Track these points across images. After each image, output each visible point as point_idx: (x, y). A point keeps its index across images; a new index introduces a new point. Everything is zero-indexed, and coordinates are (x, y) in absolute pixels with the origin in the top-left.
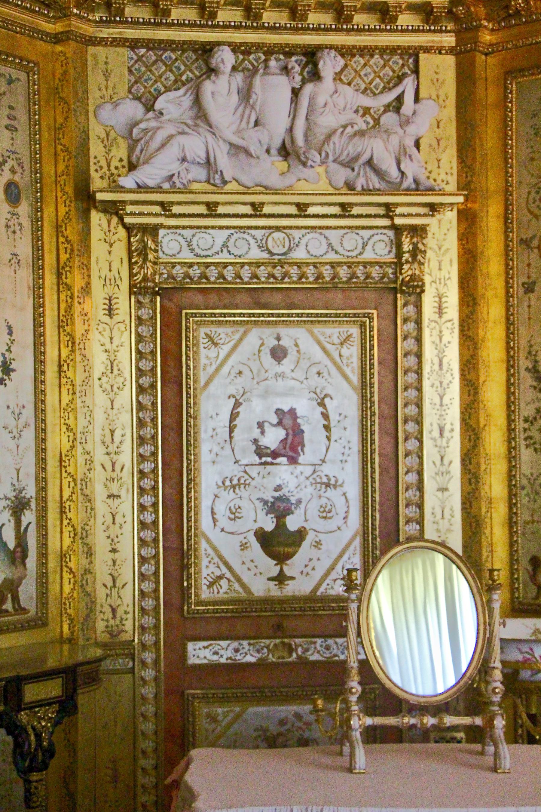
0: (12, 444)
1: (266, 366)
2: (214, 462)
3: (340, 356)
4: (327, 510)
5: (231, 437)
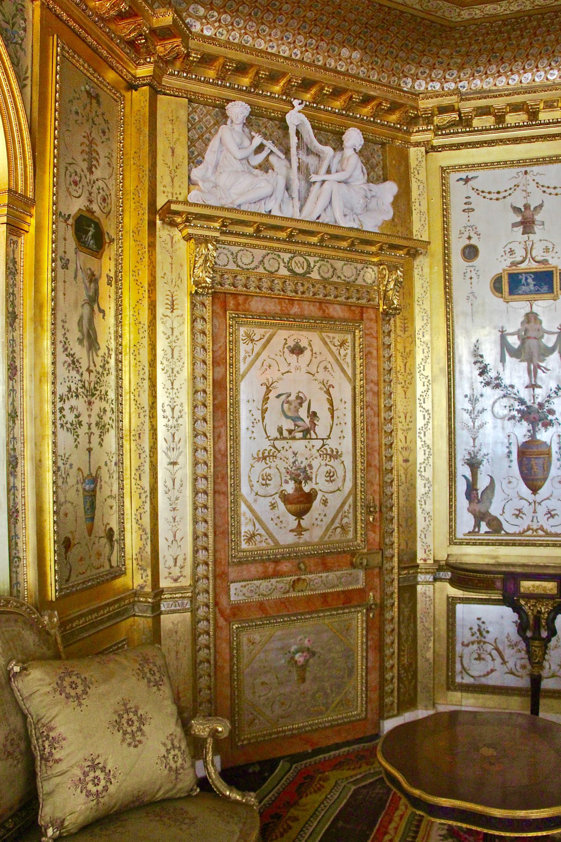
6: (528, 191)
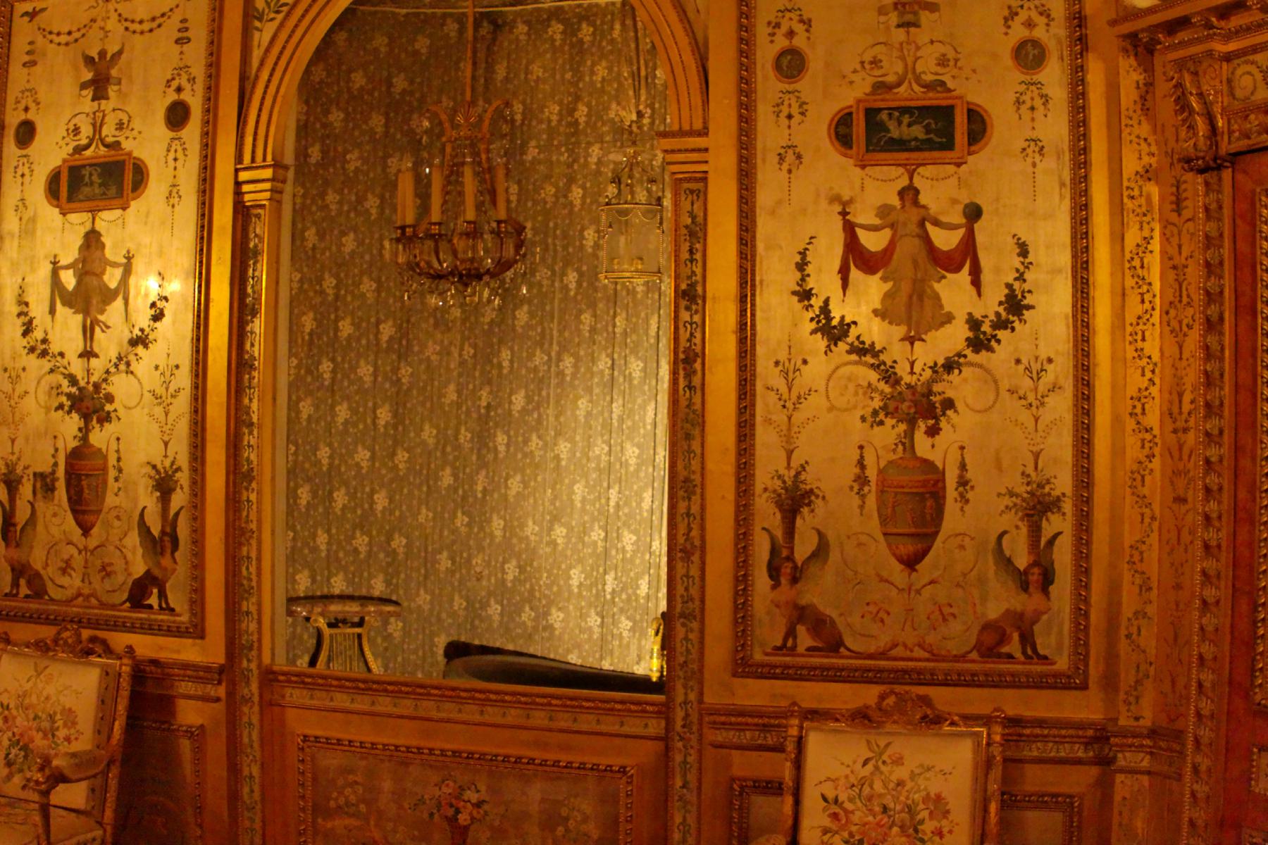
0: (1025, 417)
6: (108, 28)
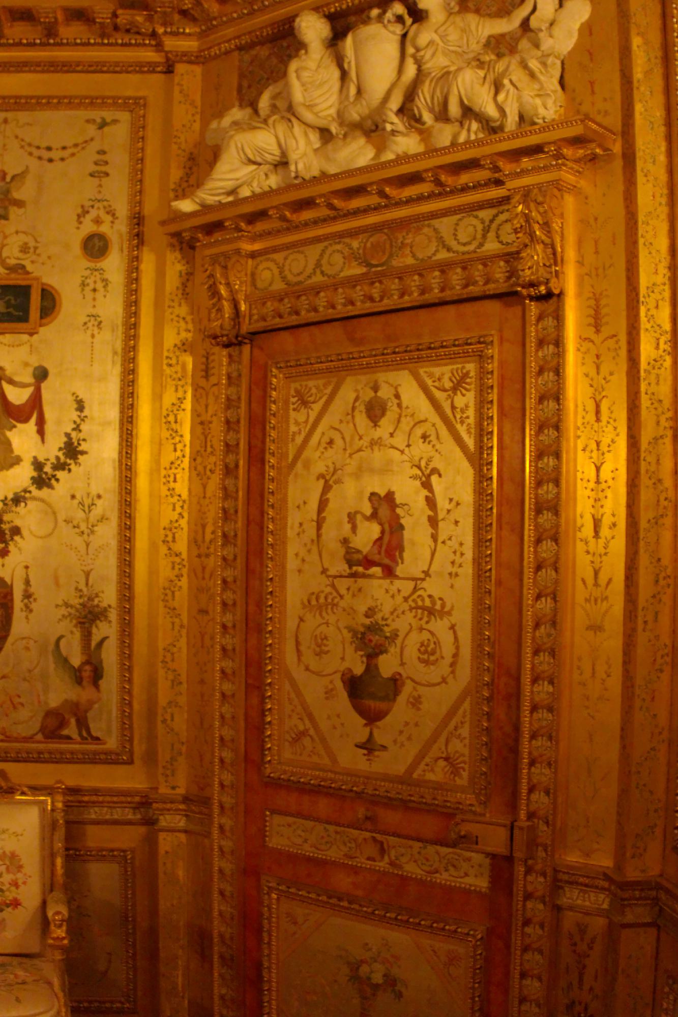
0: (79, 542)
1: (361, 431)
2: (300, 571)
3: (453, 408)
4: (429, 649)
5: (319, 536)
